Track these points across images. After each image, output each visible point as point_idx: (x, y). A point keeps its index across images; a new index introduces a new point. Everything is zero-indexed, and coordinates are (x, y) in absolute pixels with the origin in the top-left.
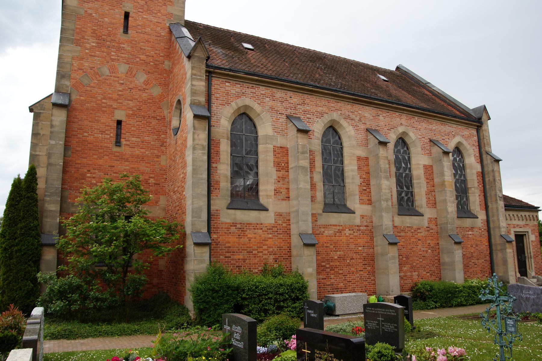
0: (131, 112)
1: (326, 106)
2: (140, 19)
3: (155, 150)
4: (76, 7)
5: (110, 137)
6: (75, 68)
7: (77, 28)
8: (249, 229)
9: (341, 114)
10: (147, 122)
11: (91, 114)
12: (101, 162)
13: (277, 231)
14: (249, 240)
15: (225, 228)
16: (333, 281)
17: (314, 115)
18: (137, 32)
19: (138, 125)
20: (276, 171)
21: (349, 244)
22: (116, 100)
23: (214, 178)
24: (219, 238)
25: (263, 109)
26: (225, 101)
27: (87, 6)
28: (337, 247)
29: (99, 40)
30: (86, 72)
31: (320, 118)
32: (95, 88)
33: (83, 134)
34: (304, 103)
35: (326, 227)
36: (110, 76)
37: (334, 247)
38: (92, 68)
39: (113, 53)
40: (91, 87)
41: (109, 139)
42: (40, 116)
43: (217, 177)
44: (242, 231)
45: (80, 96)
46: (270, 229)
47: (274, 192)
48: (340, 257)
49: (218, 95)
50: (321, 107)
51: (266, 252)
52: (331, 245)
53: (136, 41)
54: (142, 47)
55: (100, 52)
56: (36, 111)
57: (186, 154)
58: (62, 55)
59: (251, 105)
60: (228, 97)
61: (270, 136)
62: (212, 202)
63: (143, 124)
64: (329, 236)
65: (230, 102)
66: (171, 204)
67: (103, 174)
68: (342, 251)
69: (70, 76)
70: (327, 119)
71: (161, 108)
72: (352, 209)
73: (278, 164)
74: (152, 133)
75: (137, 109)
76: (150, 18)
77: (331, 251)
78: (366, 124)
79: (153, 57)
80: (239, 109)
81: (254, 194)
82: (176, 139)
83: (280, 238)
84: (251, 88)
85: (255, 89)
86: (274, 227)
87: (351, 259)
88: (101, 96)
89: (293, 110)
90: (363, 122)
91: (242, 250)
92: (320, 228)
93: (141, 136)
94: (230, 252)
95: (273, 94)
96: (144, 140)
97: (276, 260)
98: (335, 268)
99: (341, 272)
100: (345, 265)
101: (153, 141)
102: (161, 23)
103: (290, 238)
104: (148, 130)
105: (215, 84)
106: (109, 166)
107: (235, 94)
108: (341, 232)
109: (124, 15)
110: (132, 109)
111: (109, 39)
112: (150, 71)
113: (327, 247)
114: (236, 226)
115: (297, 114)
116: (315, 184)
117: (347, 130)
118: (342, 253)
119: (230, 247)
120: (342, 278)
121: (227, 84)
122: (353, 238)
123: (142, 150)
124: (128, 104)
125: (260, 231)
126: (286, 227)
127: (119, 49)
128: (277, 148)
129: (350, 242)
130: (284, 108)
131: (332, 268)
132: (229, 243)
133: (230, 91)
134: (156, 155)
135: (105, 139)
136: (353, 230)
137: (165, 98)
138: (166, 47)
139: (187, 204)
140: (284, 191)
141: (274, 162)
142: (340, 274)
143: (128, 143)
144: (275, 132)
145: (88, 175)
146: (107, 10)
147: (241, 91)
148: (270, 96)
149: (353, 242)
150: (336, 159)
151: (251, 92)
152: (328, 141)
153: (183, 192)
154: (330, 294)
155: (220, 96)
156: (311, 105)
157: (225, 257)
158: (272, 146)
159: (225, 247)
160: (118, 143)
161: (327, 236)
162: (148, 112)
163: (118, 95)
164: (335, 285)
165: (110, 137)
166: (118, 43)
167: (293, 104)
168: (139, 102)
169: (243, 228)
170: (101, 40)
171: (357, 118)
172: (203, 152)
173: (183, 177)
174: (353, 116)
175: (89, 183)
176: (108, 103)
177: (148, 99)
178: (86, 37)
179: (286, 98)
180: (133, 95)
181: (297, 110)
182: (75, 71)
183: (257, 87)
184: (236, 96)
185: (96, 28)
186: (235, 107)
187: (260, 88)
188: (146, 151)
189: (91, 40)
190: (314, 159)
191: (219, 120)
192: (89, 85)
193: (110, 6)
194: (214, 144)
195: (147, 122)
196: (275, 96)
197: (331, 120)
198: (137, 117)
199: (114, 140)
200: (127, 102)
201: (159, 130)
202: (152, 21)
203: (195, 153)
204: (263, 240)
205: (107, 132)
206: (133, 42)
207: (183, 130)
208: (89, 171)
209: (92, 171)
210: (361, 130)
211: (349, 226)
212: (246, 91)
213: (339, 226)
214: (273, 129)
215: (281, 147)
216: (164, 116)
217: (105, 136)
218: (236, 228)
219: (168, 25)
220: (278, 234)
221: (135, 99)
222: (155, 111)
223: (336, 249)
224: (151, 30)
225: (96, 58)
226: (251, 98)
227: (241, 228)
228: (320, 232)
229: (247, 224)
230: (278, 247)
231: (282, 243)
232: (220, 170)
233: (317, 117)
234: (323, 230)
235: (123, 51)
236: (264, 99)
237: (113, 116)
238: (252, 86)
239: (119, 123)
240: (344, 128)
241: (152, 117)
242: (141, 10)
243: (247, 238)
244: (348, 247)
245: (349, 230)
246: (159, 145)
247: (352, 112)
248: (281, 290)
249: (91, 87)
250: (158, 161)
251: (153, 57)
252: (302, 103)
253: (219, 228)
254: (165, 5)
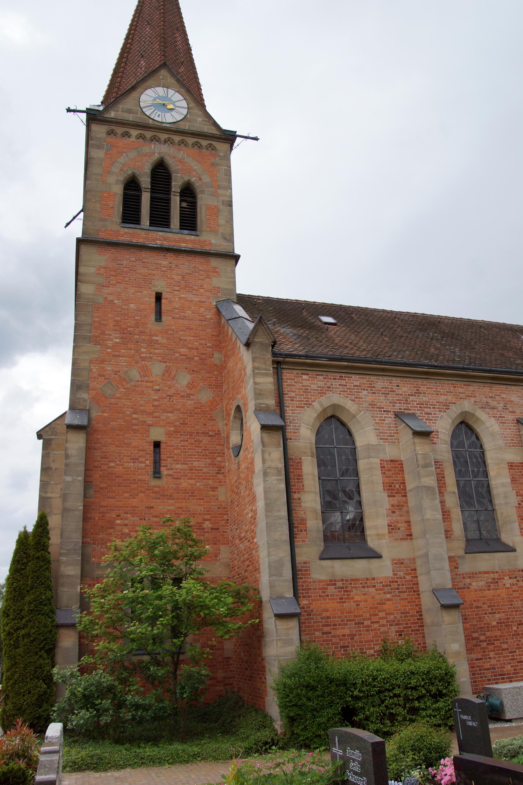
0: (172, 429)
1: (451, 392)
2: (177, 300)
3: (209, 479)
4: (92, 294)
5: (146, 466)
6: (94, 375)
7: (95, 322)
8: (356, 587)
9: (475, 402)
10: (195, 441)
11: (117, 435)
13: (398, 589)
14: (357, 605)
15: (320, 589)
16: (493, 662)
17: (434, 408)
18: (173, 318)
19: (182, 446)
20: (388, 496)
21: (512, 601)
22: (150, 414)
23: (298, 514)
24: (312, 604)
25: (360, 407)
26: (303, 401)
27: (106, 291)
28: (494, 606)
29: (123, 333)
30: (108, 379)
31: (445, 412)
32: (122, 399)
33: (108, 464)
34: (418, 393)
35: (472, 575)
36: (142, 381)
37: (489, 606)
38: (116, 372)
39: (143, 350)
40: (116, 398)
41: (144, 469)
42: (51, 444)
43: (302, 512)
44: (345, 591)
45: (103, 412)
46: (387, 586)
47: (389, 529)
48: (501, 623)
49: (293, 394)
50: (444, 395)
51: (384, 622)
52: (484, 604)
53: (173, 330)
54: (182, 338)
55: (126, 349)
56: (46, 437)
57: (254, 483)
58: (78, 358)
59: (341, 404)
60: (308, 395)
61: (373, 445)
62: (297, 550)
63: (189, 444)
64: (480, 590)
65: (312, 401)
66: (238, 557)
67: (138, 519)
68: (503, 612)
69: (88, 386)
70: (455, 411)
71: (214, 420)
72: (511, 544)
73: (390, 486)
74: (203, 455)
75: (181, 424)
76: (190, 296)
77: (486, 614)
78: (515, 412)
79: (197, 349)
80: (325, 410)
81: (359, 533)
82: (239, 462)
83: (402, 599)
84: (339, 379)
85: (346, 380)
86: (393, 582)
87: (519, 624)
88: (130, 409)
89: (404, 403)
90: (510, 409)
91: (347, 620)
92: (464, 578)
93: (189, 461)
94: (330, 625)
95: (371, 384)
96: (193, 467)
97: (400, 634)
98: (494, 640)
99: (505, 646)
100: (510, 635)
101: (205, 467)
102: (205, 302)
103: (419, 598)
104: (198, 452)
105: (287, 379)
106: (146, 507)
107: (318, 390)
108: (497, 582)
109: (154, 297)
110: (173, 423)
111: (137, 331)
112: (195, 369)
113: (477, 607)
114: (335, 584)
115: (410, 410)
116: (449, 511)
117: (488, 424)
118: (502, 615)
119: (328, 618)
120: (508, 656)
121: (304, 377)
122: (518, 591)
123: (191, 481)
124: (168, 418)
125: (372, 590)
126: (412, 581)
127: (151, 343)
128: (385, 463)
129: (514, 598)
130: (390, 403)
131: (491, 641)
132: (327, 611)
133: (310, 386)
134: (210, 488)
135: (138, 469)
136: (516, 578)
137: (219, 404)
138: (214, 333)
139: (261, 556)
140: (402, 526)
141: (383, 483)
142: (504, 650)
143: (171, 472)
144: (381, 439)
145: (118, 522)
146: (133, 294)
147: (325, 384)
148: (368, 387)
149: (518, 597)
150: (476, 469)
151: (339, 385)
152: (461, 444)
153: (253, 538)
154: (492, 684)
155: (296, 395)
156: (428, 394)
157: (323, 633)
158: (378, 461)
159: (322, 618)
160: (157, 474)
161: (475, 590)
162: (196, 427)
163: (153, 406)
164: (498, 668)
165: (146, 466)
166: (149, 335)
167: (402, 395)
168: (182, 413)
169: (346, 587)
170: (126, 334)
171: (501, 405)
172: (279, 477)
173: (252, 517)
174: (494, 403)
175: (120, 533)
176: (140, 419)
177: (195, 408)
178: (107, 332)
179: (391, 388)
180: (174, 404)
181: (410, 404)
182: (95, 378)
183: (348, 377)
184: (319, 393)
185: (119, 319)
186: (319, 409)
187: (351, 377)
188: (197, 482)
189: (114, 335)
190: (444, 474)
191: (298, 429)
192: (114, 395)
193: (136, 287)
194: (293, 466)
195: (195, 441)
196: (374, 387)
197: (462, 413)
198: (181, 435)
199: (150, 470)
200: (165, 414)
201: (213, 450)
202: (192, 301)
203: (267, 481)
204: (378, 604)
205: (140, 459)
206: (169, 332)
207: (247, 449)
208: (119, 516)
209: (123, 515)
210: (508, 423)
211: (509, 571)
212: (332, 385)
213: (493, 572)
214: (377, 436)
215: (391, 461)
216: (219, 431)
217: (138, 466)
218: (335, 588)
219: (215, 304)
220: (399, 592)
221: (177, 410)
222: (205, 425)
223: (492, 610)
224: (192, 313)
225: (121, 358)
226: (340, 394)
227: (342, 588)
228: (465, 584)
229: (352, 580)
230: (402, 613)
231: (408, 606)
232: (305, 502)
233: (440, 411)
234: (468, 581)
235: (156, 346)
236: (359, 392)
237: (148, 436)
238: (340, 377)
239: (157, 445)
240: (483, 423)
241: (202, 433)
242: (177, 288)
243: (354, 602)
244: (512, 605)
245: (510, 578)
246: (215, 472)
247: (491, 397)
248: (413, 682)
249: (116, 398)
250: (214, 496)
251: (197, 349)
252: (415, 393)
253: (310, 589)
254: (208, 277)
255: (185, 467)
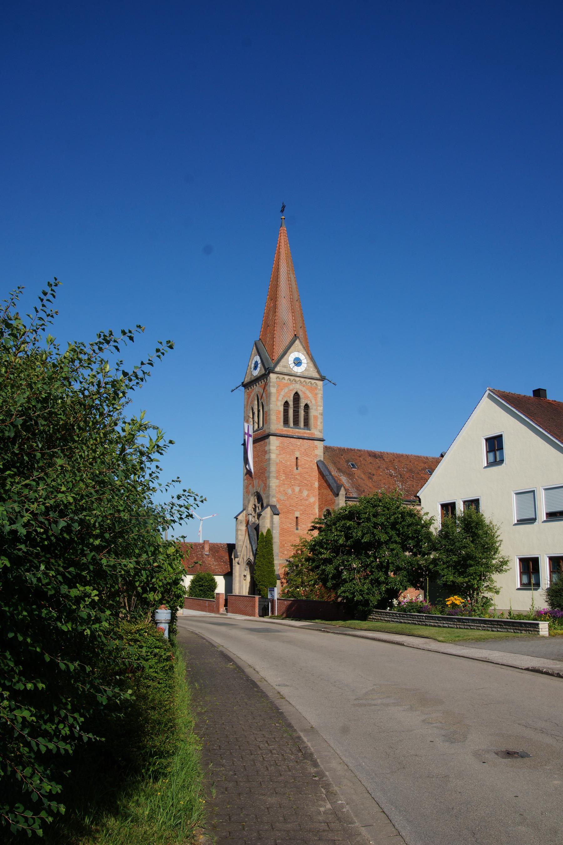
0: (302, 512)
12: (290, 538)
127: (295, 479)
143: (301, 528)
209: (287, 543)
239: (297, 518)
255: (306, 526)
